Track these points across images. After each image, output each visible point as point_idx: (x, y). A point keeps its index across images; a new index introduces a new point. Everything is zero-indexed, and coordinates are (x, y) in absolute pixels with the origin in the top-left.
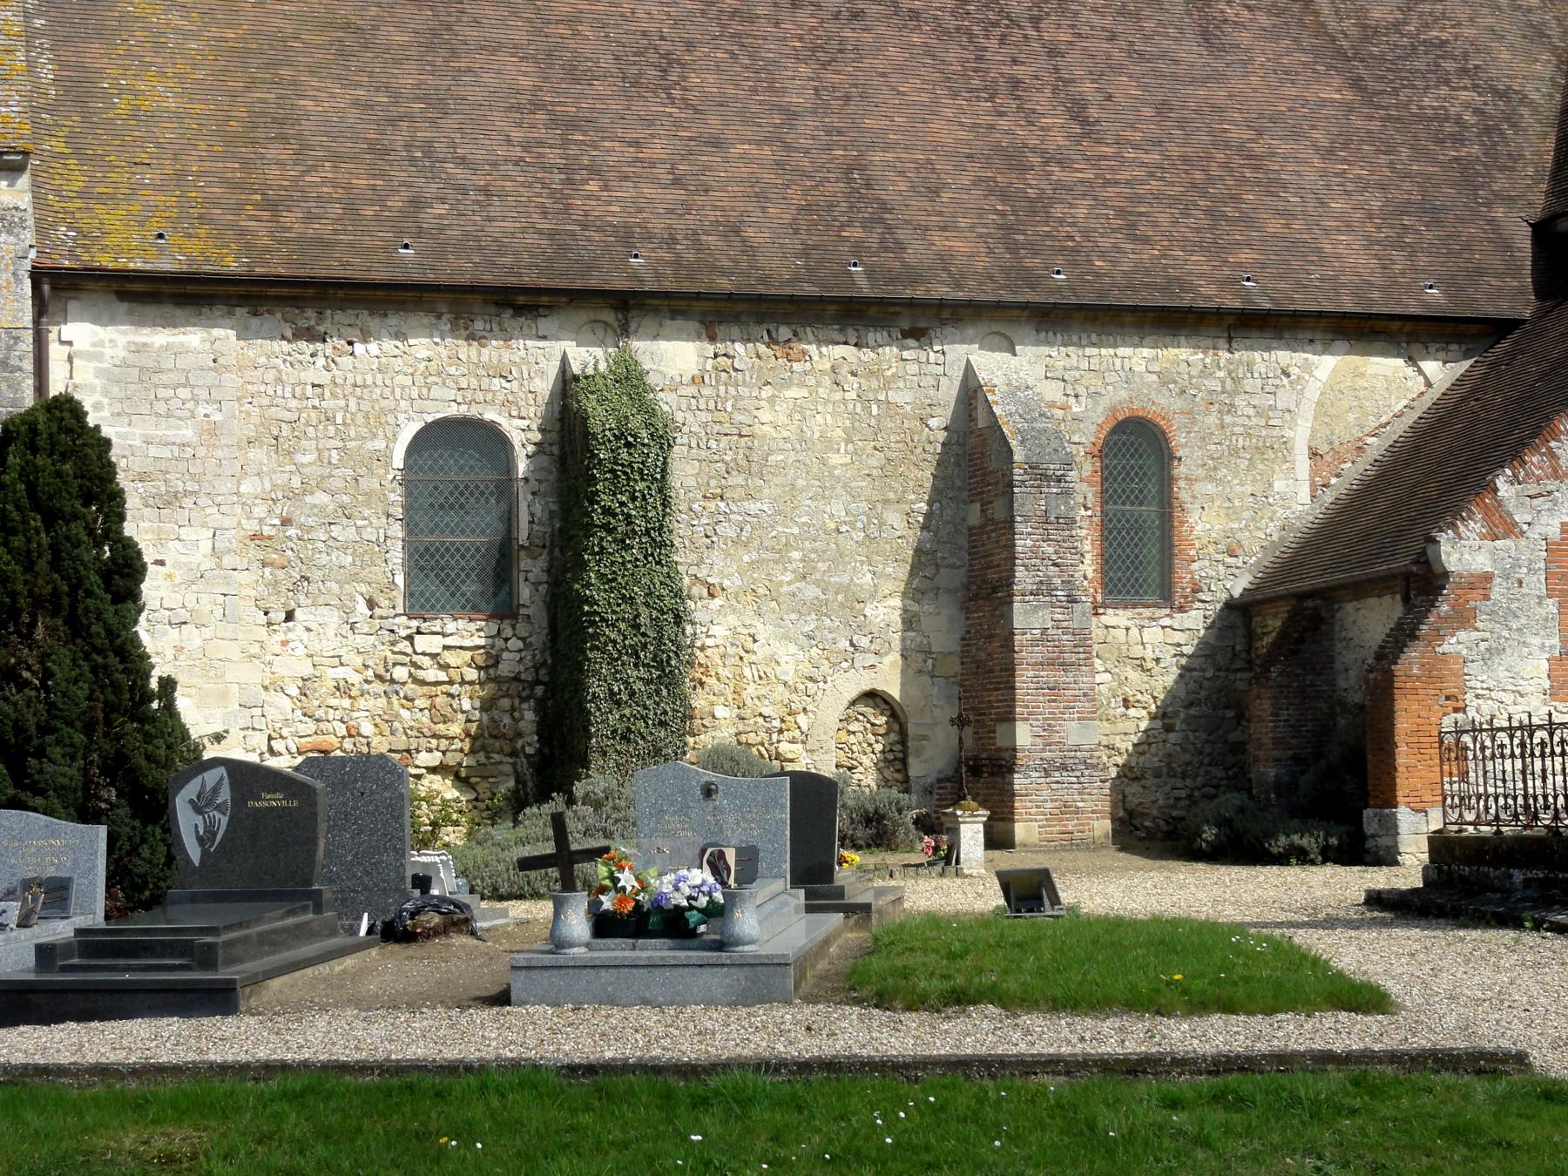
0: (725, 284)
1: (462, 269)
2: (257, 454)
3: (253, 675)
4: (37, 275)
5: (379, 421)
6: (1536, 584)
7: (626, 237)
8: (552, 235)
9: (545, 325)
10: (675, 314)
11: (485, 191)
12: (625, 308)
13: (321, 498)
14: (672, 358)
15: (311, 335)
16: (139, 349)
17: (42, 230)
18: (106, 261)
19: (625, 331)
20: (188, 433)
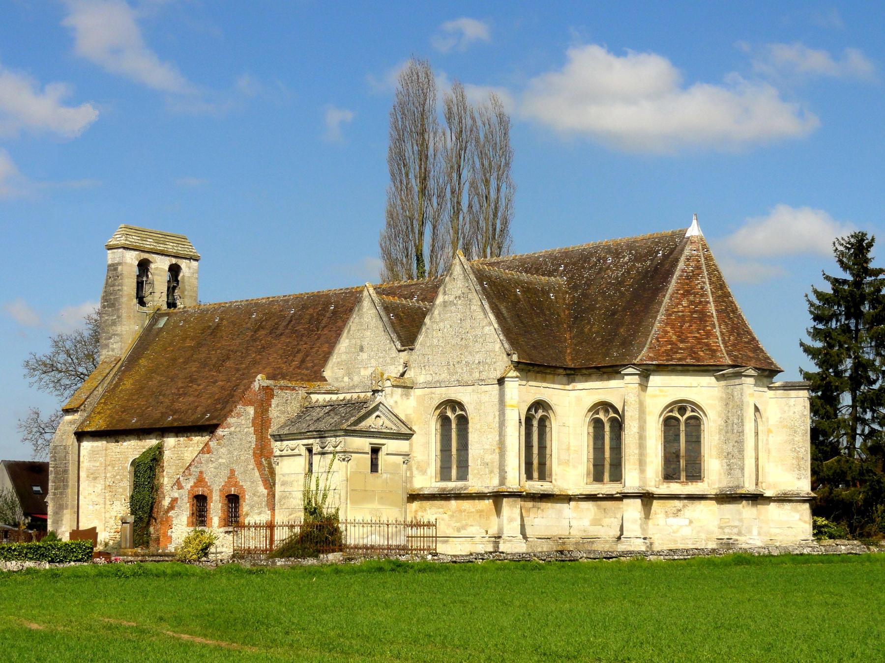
0: (176, 424)
1: (138, 426)
2: (109, 468)
3: (108, 515)
4: (76, 434)
5: (127, 461)
6: (186, 499)
7: (175, 412)
8: (162, 413)
9: (151, 436)
10: (171, 432)
11: (162, 403)
12: (163, 432)
13: (118, 477)
14: (170, 442)
15: (118, 442)
16: (92, 447)
17: (82, 423)
18: (86, 430)
19: (163, 437)
20: (98, 464)
